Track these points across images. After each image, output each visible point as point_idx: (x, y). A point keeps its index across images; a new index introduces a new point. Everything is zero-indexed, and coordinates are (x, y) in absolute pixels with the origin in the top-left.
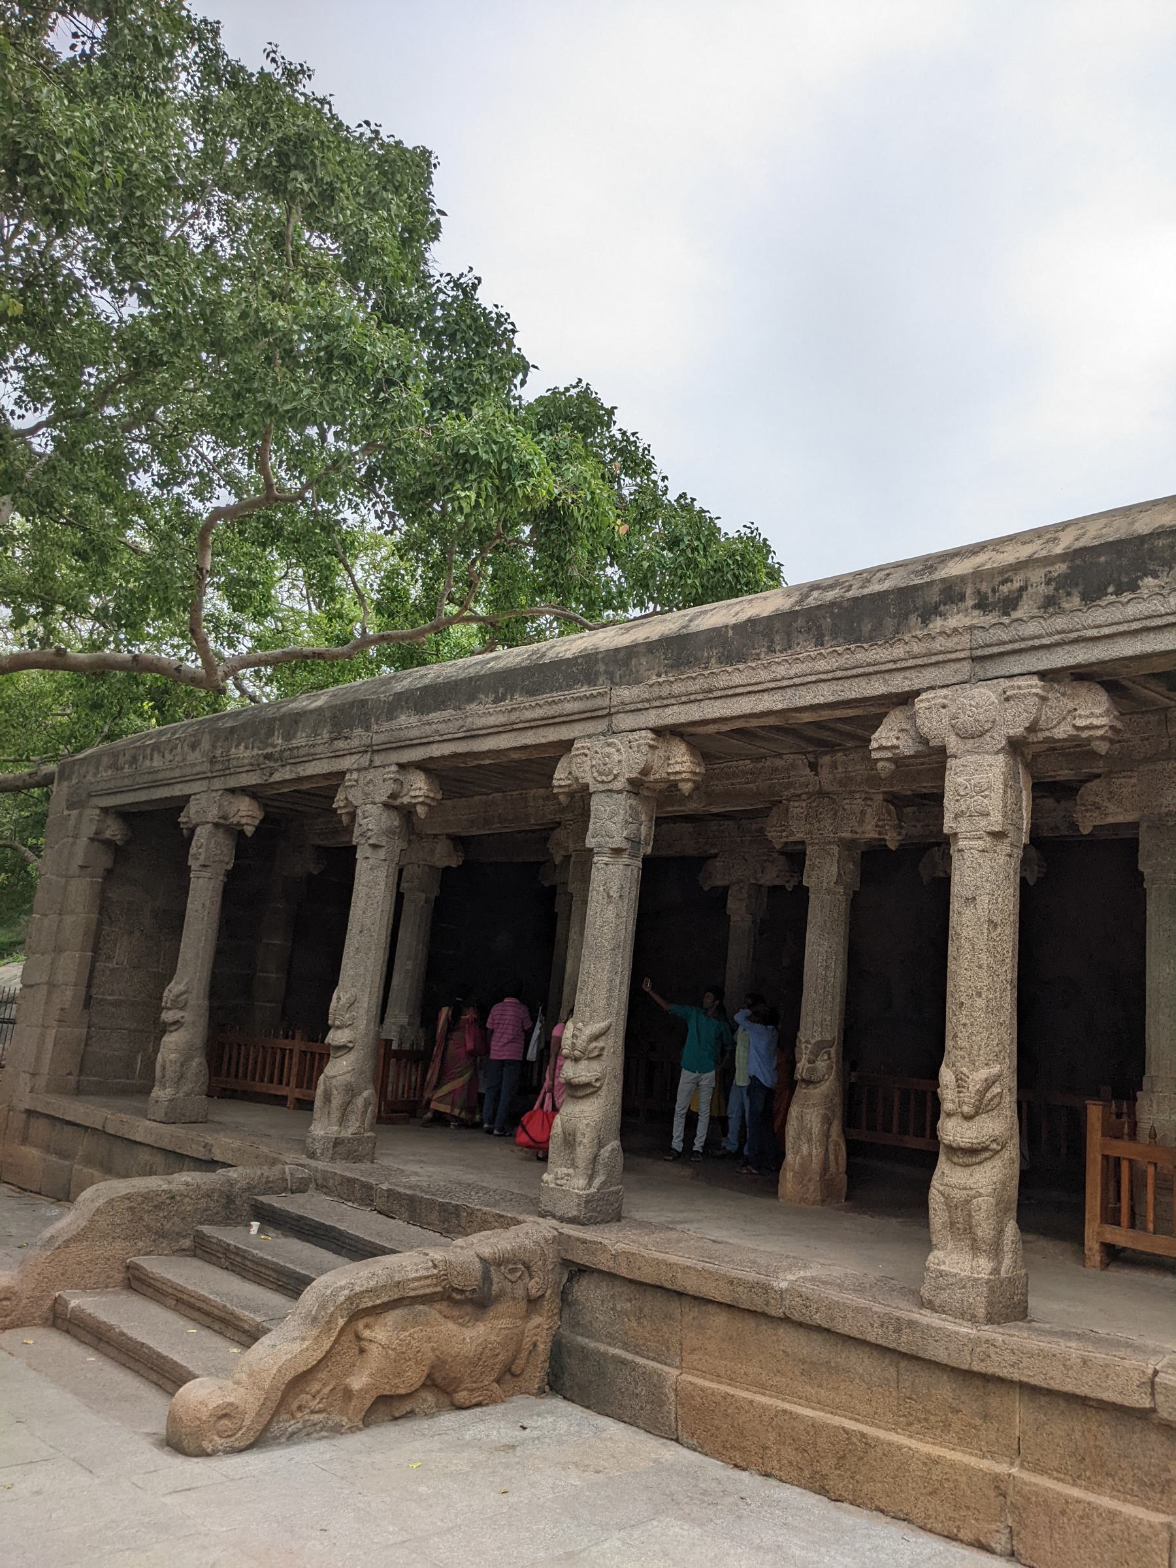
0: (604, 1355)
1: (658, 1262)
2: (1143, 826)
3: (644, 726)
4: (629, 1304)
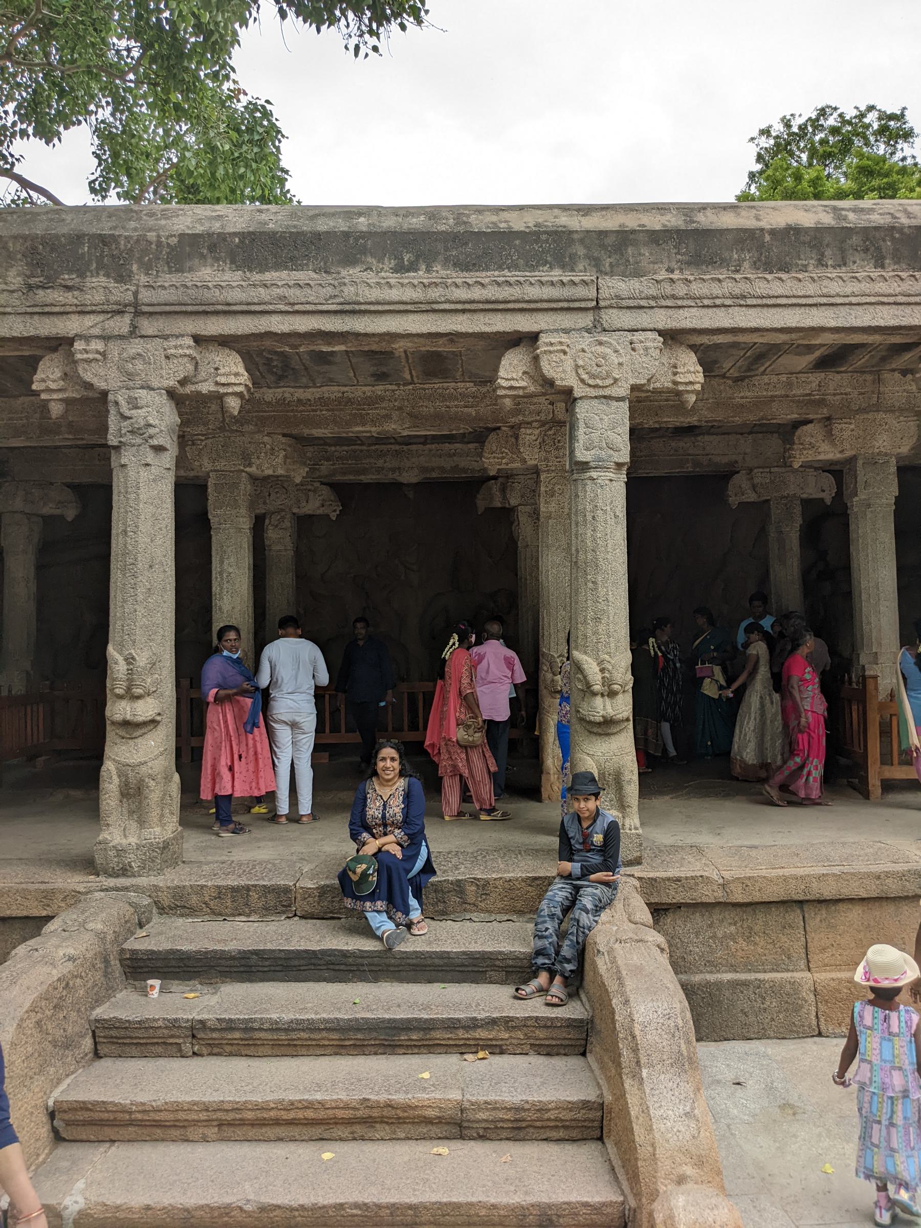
0: (718, 985)
1: (785, 879)
2: (860, 462)
3: (651, 326)
4: (733, 928)
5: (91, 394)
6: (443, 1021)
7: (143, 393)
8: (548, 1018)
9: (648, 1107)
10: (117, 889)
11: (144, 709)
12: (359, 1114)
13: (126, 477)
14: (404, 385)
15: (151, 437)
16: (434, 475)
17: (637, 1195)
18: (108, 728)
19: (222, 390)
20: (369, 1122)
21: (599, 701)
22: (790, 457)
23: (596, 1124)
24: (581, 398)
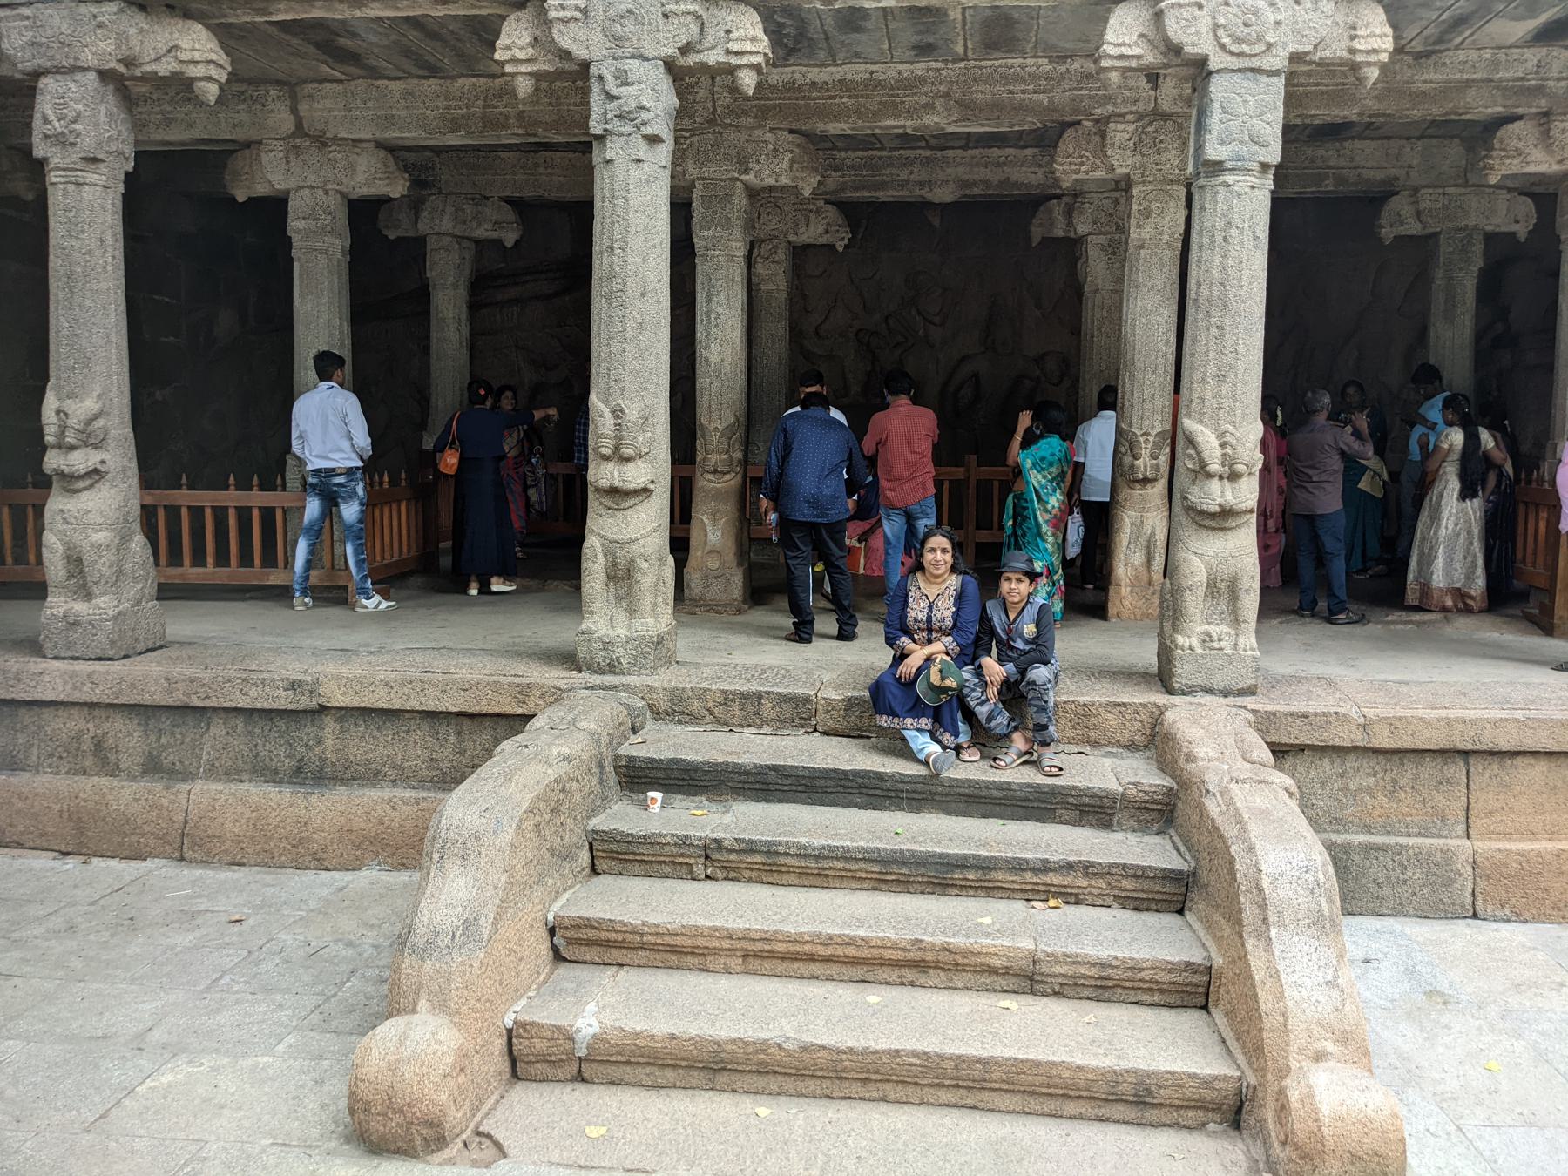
1: (1449, 722)
4: (1371, 780)
5: (569, 67)
6: (1007, 860)
7: (635, 63)
8: (1138, 867)
9: (1277, 972)
10: (604, 688)
11: (635, 475)
12: (910, 956)
13: (612, 176)
14: (954, 62)
15: (644, 124)
16: (976, 191)
17: (1261, 1071)
18: (590, 496)
19: (734, 61)
20: (921, 966)
21: (1215, 485)
22: (1485, 168)
23: (1200, 990)
24: (1218, 71)
